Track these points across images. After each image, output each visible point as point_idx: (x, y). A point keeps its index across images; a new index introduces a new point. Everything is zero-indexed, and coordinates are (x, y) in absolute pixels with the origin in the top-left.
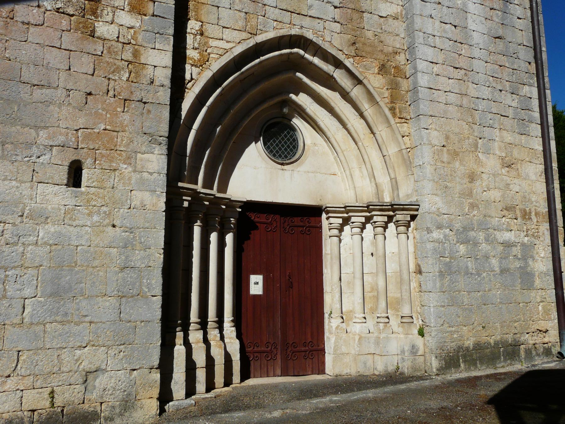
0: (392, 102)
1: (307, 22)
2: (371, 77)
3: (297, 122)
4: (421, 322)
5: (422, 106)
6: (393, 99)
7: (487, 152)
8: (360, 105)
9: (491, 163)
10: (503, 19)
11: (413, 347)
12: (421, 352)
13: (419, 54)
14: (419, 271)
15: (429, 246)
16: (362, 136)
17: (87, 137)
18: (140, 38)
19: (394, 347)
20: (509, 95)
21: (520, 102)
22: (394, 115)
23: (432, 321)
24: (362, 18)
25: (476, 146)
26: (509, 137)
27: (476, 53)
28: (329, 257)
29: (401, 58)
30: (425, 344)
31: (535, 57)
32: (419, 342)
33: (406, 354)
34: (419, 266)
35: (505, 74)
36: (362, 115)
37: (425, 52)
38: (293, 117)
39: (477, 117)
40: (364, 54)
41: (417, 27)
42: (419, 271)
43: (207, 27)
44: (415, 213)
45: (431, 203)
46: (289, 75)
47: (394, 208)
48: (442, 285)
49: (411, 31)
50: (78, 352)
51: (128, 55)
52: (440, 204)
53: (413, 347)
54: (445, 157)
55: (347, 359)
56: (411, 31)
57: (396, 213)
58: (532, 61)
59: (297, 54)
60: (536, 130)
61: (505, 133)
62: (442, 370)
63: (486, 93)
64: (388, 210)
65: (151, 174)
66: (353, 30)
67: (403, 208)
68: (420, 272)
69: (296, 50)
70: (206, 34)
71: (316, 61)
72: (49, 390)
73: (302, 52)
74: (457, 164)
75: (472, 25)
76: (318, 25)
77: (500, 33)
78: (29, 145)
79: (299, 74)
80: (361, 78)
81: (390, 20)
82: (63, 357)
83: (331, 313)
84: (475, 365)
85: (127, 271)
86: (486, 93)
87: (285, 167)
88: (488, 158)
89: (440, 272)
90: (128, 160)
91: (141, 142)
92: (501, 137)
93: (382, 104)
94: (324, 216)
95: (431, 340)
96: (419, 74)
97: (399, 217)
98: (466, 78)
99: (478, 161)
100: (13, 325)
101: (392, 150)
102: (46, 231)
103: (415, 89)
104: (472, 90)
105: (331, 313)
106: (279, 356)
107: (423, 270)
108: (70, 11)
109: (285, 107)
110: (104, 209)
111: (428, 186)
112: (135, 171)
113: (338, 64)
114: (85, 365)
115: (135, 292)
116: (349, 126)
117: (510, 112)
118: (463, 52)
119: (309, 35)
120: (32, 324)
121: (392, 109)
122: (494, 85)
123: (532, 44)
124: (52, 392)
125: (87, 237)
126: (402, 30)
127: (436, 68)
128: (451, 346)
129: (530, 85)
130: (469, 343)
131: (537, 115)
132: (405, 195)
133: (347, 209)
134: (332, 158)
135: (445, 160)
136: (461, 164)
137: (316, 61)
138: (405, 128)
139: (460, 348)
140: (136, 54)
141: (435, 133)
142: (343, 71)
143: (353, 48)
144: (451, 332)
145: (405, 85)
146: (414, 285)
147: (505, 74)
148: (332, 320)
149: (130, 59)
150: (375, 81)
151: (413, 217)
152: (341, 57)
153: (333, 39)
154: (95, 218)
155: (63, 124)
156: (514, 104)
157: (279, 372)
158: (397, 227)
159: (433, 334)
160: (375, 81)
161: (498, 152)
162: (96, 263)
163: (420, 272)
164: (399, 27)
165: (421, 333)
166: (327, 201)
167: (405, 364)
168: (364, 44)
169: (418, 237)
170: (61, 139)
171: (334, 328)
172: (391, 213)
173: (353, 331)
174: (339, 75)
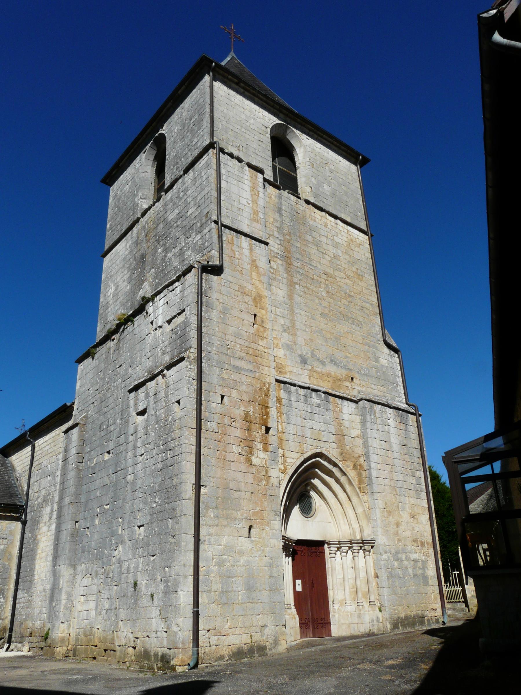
0: (359, 484)
1: (322, 444)
2: (350, 471)
3: (312, 493)
4: (379, 605)
5: (374, 488)
6: (360, 482)
7: (403, 510)
8: (345, 486)
9: (405, 516)
10: (406, 435)
11: (377, 618)
12: (381, 621)
13: (371, 460)
14: (377, 576)
15: (382, 563)
16: (345, 502)
17: (254, 514)
18: (267, 463)
19: (367, 619)
20: (411, 477)
21: (416, 481)
22: (360, 491)
23: (386, 604)
24: (344, 439)
25: (398, 508)
26: (413, 501)
27: (396, 455)
28: (330, 569)
29: (362, 460)
30: (382, 616)
31: (421, 454)
32: (380, 615)
33: (375, 622)
34: (377, 574)
35: (409, 465)
36: (345, 491)
37: (374, 458)
38: (310, 490)
39: (398, 491)
40: (346, 459)
41: (370, 444)
42: (377, 576)
43: (286, 452)
44: (373, 545)
45: (381, 540)
46: (313, 470)
47: (363, 542)
48: (389, 583)
49: (366, 444)
50: (258, 617)
51: (264, 473)
52: (385, 540)
53: (377, 618)
54: (386, 514)
55: (344, 627)
56: (366, 444)
57: (364, 544)
58: (420, 456)
59: (318, 461)
60: (424, 495)
61: (411, 499)
62: (393, 629)
63: (401, 477)
64: (360, 543)
65: (276, 530)
66: (341, 446)
67: (368, 542)
68: (377, 577)
69: (317, 459)
70: (285, 456)
71: (325, 463)
72: (250, 634)
73: (320, 460)
74: (391, 518)
75: (393, 440)
76: (327, 445)
77: (405, 443)
78: (235, 519)
79: (317, 470)
80: (346, 472)
81: (356, 439)
82: (253, 619)
83: (333, 601)
84: (406, 628)
85: (272, 578)
86: (401, 477)
87: (309, 519)
88: (404, 513)
89: (388, 576)
90: (268, 524)
91: (272, 515)
92: (409, 501)
93: (355, 486)
94: (326, 546)
95: (386, 614)
96: (372, 470)
97: (366, 547)
98: (392, 470)
99: (400, 516)
100: (236, 604)
101: (360, 510)
102: (243, 560)
103: (370, 477)
104: (395, 478)
105: (333, 601)
106: (311, 626)
107: (379, 575)
108: (243, 453)
109: (308, 486)
110: (262, 548)
111: (380, 531)
112: (271, 529)
113: (335, 465)
114: (260, 623)
115: (275, 588)
116: (339, 497)
117: (412, 487)
118: (390, 456)
119: (325, 452)
120: (242, 603)
121: (359, 488)
122: (404, 472)
123: (419, 448)
124: (251, 636)
125: (257, 562)
126: (361, 443)
127: (379, 465)
128: (395, 617)
129: (420, 471)
130: (403, 615)
131: (424, 487)
132: (367, 535)
133: (340, 543)
134: (328, 513)
135: (386, 516)
136: (393, 518)
137: (325, 463)
138: (365, 498)
139: (399, 618)
140: (267, 472)
141: (380, 502)
142: (337, 468)
143: (342, 456)
144: (394, 609)
145: (364, 474)
146: (374, 584)
147: (409, 465)
148: (334, 605)
149: (265, 474)
150: (352, 473)
151: (372, 547)
152: (337, 462)
153: (333, 453)
154: (259, 553)
155: (245, 508)
156: (414, 482)
157: (312, 636)
158: (364, 553)
159: (387, 610)
160: (352, 473)
161: (408, 510)
162: (261, 575)
163: (377, 577)
164: (359, 442)
165: (380, 610)
166: (327, 539)
167: (374, 627)
168: (346, 454)
169: (375, 558)
170: (245, 516)
171: (337, 609)
172: (361, 545)
173: (346, 610)
174: (335, 470)
